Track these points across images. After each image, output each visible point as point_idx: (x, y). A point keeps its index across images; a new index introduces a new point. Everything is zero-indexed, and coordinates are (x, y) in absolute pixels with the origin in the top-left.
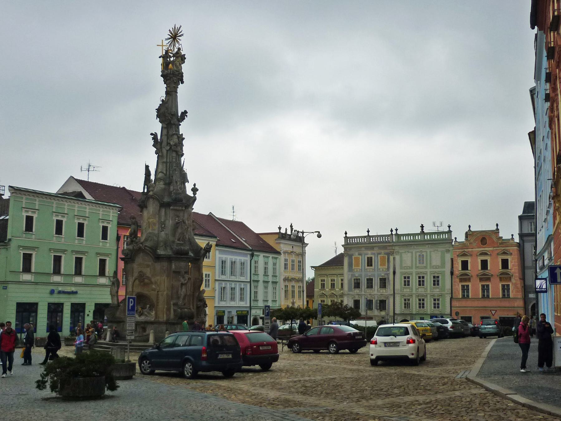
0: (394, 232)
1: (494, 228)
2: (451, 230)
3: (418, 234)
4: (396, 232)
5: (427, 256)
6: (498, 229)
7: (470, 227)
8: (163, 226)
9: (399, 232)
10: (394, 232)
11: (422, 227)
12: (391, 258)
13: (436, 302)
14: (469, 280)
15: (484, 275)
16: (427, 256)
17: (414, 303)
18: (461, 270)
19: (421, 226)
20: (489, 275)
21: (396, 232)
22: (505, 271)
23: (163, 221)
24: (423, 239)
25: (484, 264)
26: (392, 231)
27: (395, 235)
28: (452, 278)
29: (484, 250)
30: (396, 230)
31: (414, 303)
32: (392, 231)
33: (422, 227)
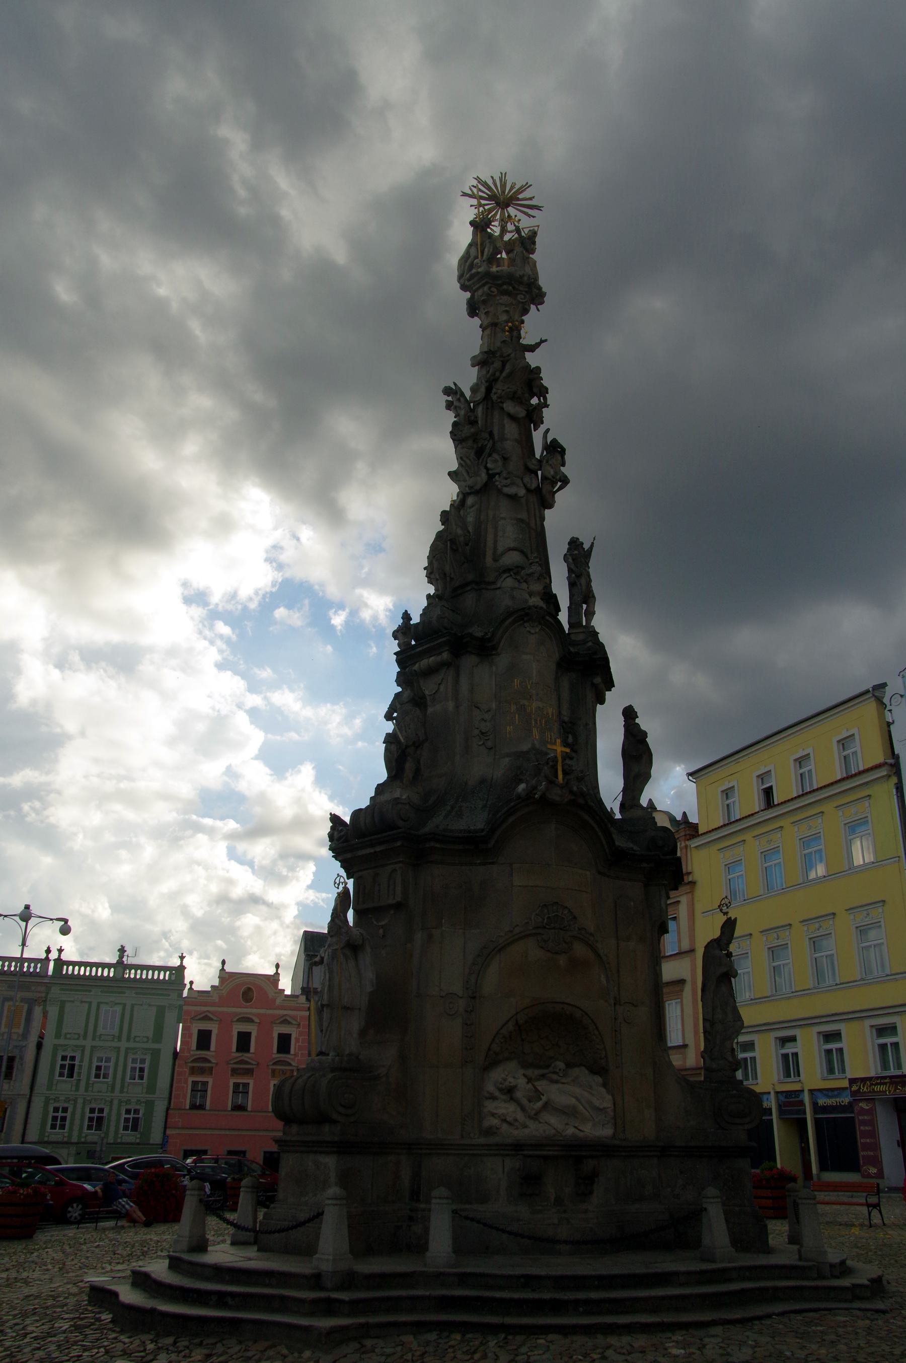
0: (54, 955)
1: (271, 971)
2: (184, 964)
3: (109, 966)
4: (59, 956)
5: (123, 1015)
6: (277, 974)
7: (224, 962)
8: (570, 739)
9: (64, 957)
10: (54, 955)
11: (122, 950)
12: (38, 1011)
13: (60, 1114)
14: (249, 1072)
15: (242, 1062)
16: (123, 1015)
17: (78, 1116)
18: (195, 1048)
19: (119, 950)
20: (250, 1064)
21: (59, 956)
22: (282, 1056)
23: (566, 719)
24: (119, 976)
25: (244, 1041)
26: (48, 951)
27: (55, 960)
28: (174, 1065)
29: (246, 1013)
30: (60, 951)
31: (78, 1116)
32: (48, 951)
33: (122, 950)
